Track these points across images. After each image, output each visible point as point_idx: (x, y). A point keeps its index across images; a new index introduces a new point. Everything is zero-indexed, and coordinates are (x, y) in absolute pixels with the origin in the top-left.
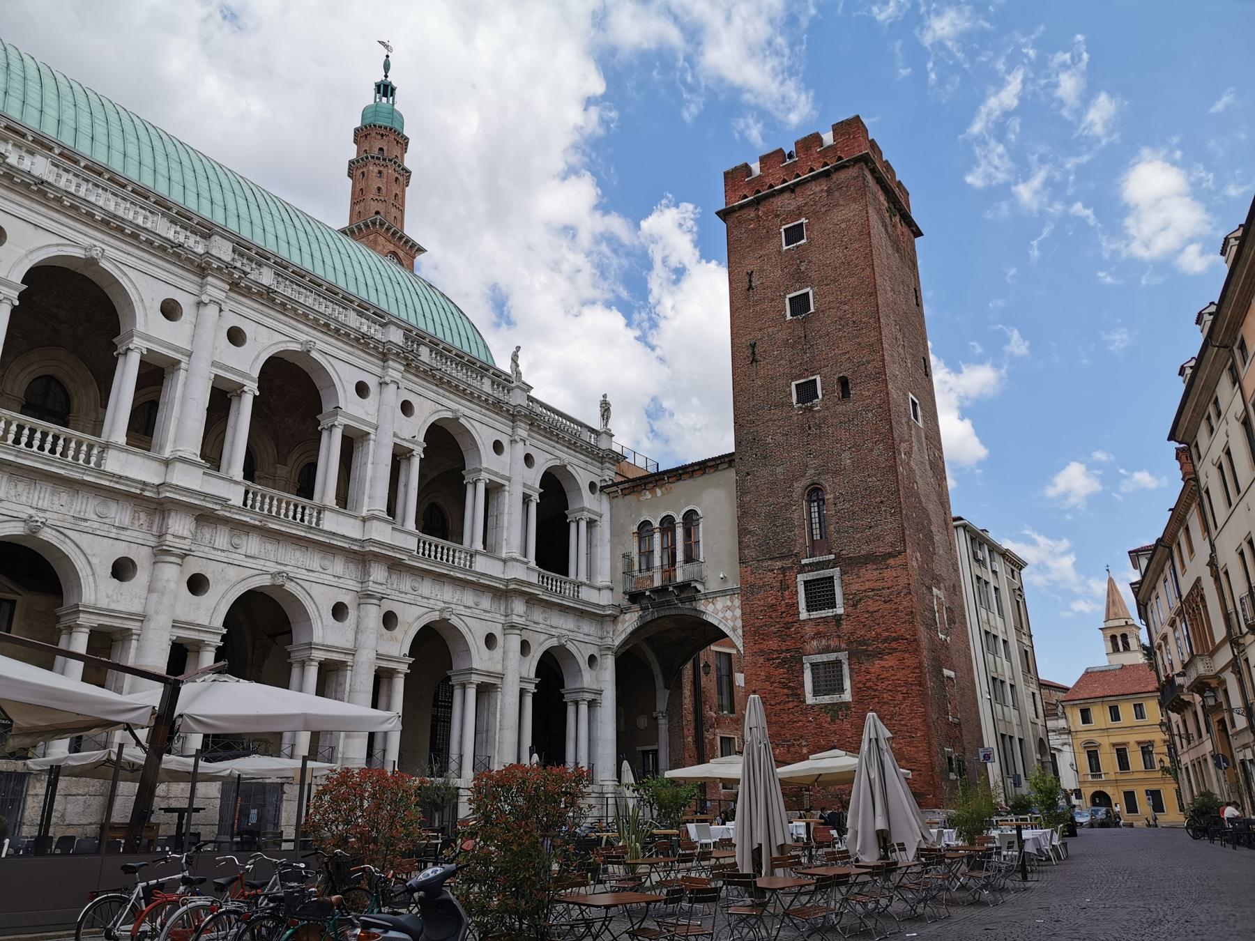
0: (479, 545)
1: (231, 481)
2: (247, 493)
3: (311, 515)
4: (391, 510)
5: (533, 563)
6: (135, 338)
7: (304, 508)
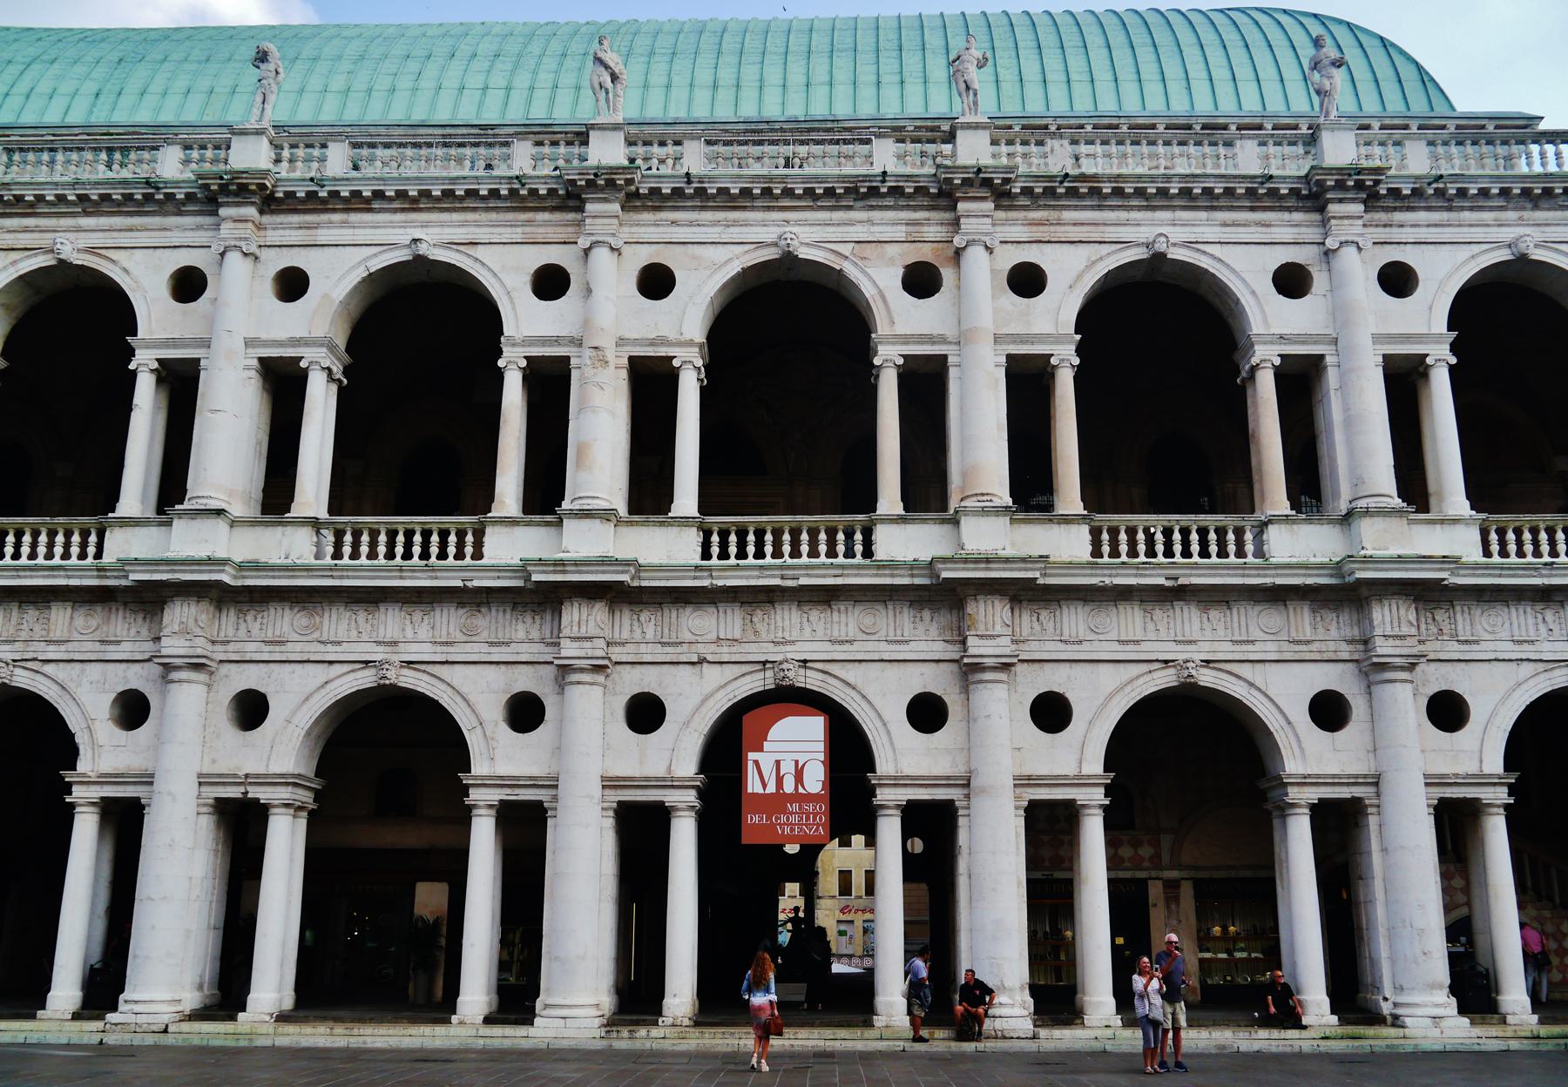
1: (1455, 521)
2: (1484, 534)
6: (1256, 347)
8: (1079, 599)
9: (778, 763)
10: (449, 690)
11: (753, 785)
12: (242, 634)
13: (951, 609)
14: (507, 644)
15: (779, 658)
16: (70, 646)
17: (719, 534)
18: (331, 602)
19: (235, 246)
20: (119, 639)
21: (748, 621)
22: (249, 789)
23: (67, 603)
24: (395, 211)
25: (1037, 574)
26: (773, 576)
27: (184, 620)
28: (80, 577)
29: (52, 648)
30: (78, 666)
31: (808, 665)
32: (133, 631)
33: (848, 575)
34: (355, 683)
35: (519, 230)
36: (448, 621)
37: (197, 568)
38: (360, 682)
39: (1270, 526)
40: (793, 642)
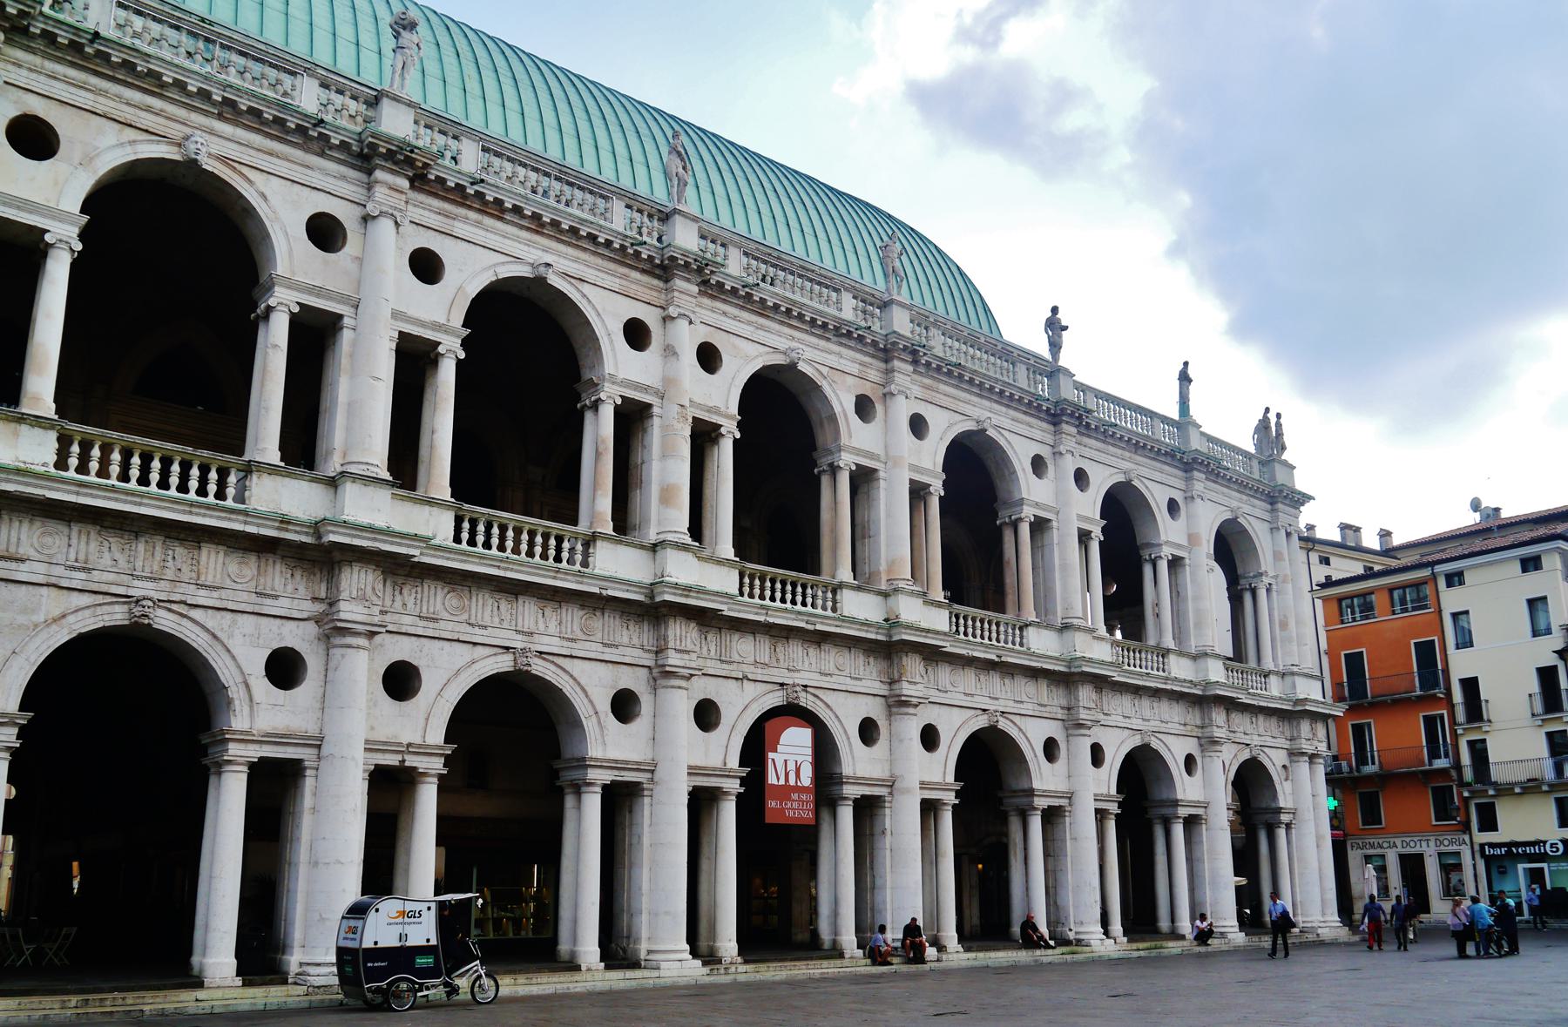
0: (845, 574)
3: (572, 550)
4: (696, 530)
5: (939, 594)
7: (559, 540)
8: (947, 662)
9: (786, 761)
10: (571, 681)
11: (772, 779)
12: (398, 605)
13: (884, 659)
14: (617, 646)
15: (790, 682)
16: (223, 594)
17: (200, 468)
18: (479, 588)
19: (392, 215)
20: (278, 594)
21: (772, 650)
22: (406, 757)
23: (220, 547)
24: (522, 227)
25: (947, 644)
26: (802, 620)
27: (363, 587)
28: (258, 525)
29: (202, 592)
30: (229, 615)
31: (808, 689)
32: (290, 588)
33: (844, 627)
34: (496, 666)
35: (617, 280)
36: (573, 618)
37: (398, 540)
38: (500, 665)
39: (1029, 628)
40: (798, 671)
